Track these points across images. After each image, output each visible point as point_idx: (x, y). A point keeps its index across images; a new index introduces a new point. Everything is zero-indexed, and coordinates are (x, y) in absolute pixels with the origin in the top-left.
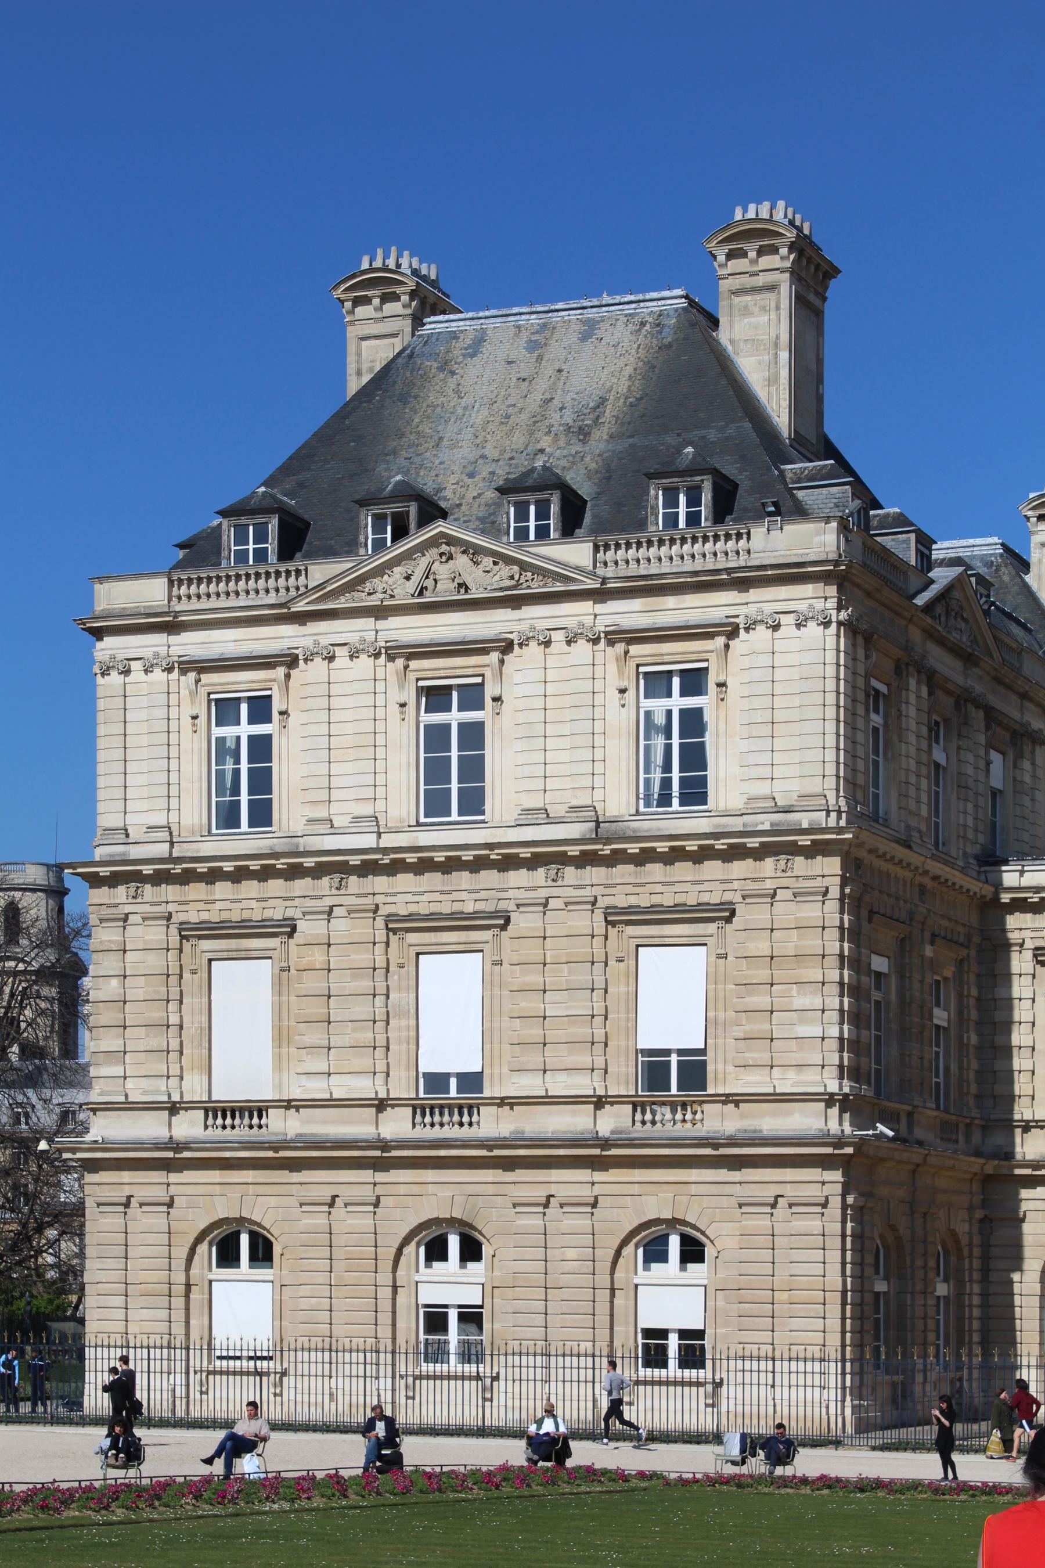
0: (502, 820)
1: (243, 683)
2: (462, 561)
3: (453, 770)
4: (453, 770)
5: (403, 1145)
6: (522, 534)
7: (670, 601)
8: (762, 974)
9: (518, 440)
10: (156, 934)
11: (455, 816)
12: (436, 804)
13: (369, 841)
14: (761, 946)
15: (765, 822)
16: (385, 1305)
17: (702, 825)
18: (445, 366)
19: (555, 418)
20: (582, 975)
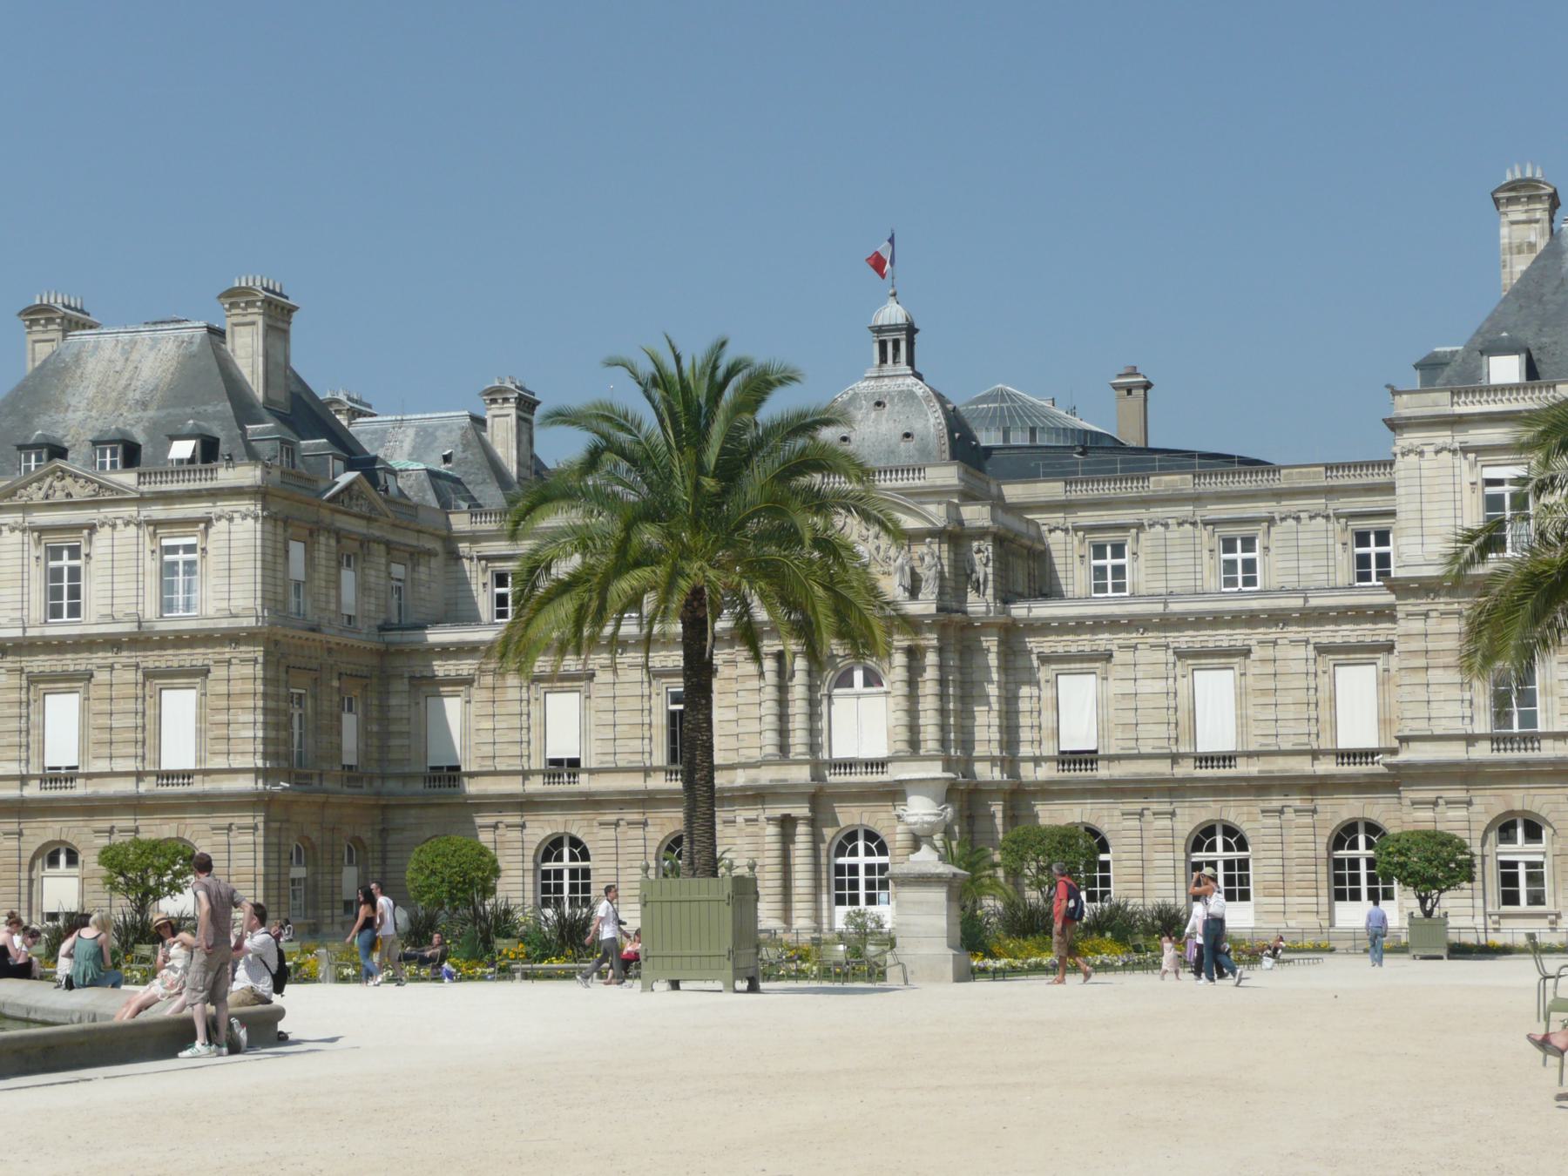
0: (90, 623)
2: (69, 481)
3: (64, 593)
4: (64, 593)
5: (33, 800)
6: (103, 465)
8: (224, 703)
9: (110, 407)
11: (65, 619)
12: (55, 612)
13: (18, 633)
14: (223, 688)
15: (224, 624)
16: (25, 890)
17: (192, 625)
19: (130, 395)
20: (131, 705)
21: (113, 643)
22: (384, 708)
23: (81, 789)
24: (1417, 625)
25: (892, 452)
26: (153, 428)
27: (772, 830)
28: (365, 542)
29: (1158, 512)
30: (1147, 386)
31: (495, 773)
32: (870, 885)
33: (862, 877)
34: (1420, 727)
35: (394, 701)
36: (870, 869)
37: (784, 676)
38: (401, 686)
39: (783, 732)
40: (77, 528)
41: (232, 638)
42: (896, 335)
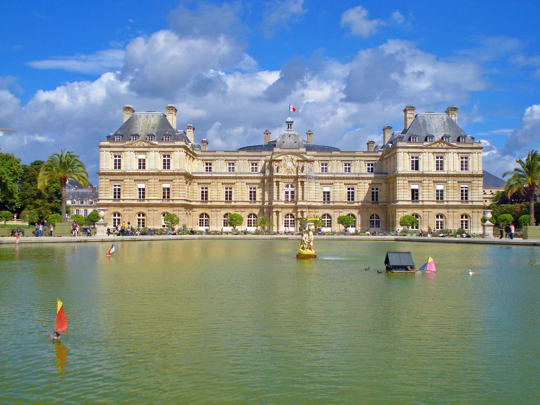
0: (147, 170)
4: (142, 164)
10: (107, 180)
12: (140, 168)
14: (175, 184)
21: (153, 174)
23: (146, 202)
24: (400, 182)
25: (292, 145)
26: (157, 133)
27: (275, 213)
29: (333, 158)
32: (291, 224)
33: (289, 222)
34: (400, 199)
36: (291, 221)
37: (278, 185)
40: (146, 152)
41: (178, 174)
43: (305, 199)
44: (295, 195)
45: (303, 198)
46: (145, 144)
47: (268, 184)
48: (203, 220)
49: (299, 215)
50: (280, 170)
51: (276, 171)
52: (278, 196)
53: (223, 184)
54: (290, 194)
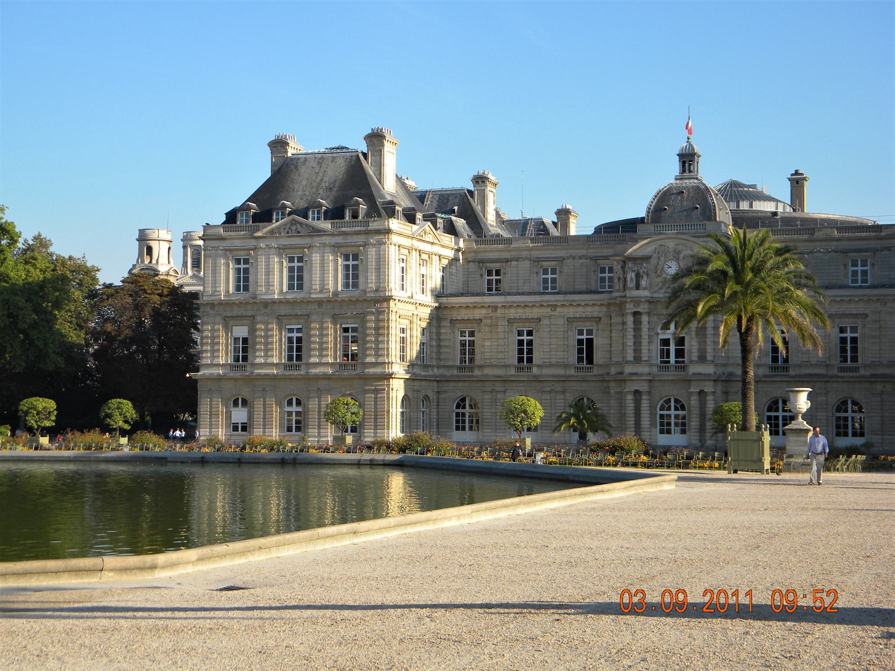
1: (242, 255)
2: (298, 225)
7: (349, 237)
9: (314, 190)
18: (296, 167)
19: (323, 185)
21: (320, 303)
22: (439, 334)
27: (630, 397)
28: (430, 255)
30: (805, 179)
31: (492, 366)
33: (673, 421)
35: (443, 331)
37: (637, 323)
38: (446, 323)
39: (637, 350)
42: (690, 158)
43: (709, 357)
44: (686, 347)
45: (702, 359)
46: (299, 228)
47: (620, 320)
48: (464, 415)
49: (694, 401)
50: (643, 283)
51: (631, 284)
52: (637, 350)
53: (511, 321)
54: (672, 348)
